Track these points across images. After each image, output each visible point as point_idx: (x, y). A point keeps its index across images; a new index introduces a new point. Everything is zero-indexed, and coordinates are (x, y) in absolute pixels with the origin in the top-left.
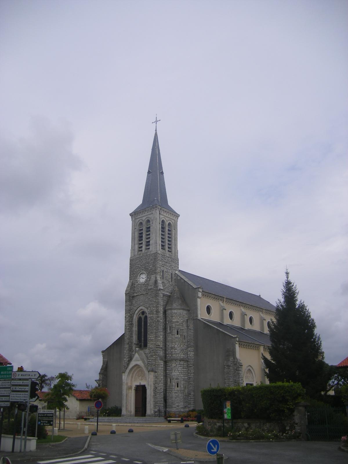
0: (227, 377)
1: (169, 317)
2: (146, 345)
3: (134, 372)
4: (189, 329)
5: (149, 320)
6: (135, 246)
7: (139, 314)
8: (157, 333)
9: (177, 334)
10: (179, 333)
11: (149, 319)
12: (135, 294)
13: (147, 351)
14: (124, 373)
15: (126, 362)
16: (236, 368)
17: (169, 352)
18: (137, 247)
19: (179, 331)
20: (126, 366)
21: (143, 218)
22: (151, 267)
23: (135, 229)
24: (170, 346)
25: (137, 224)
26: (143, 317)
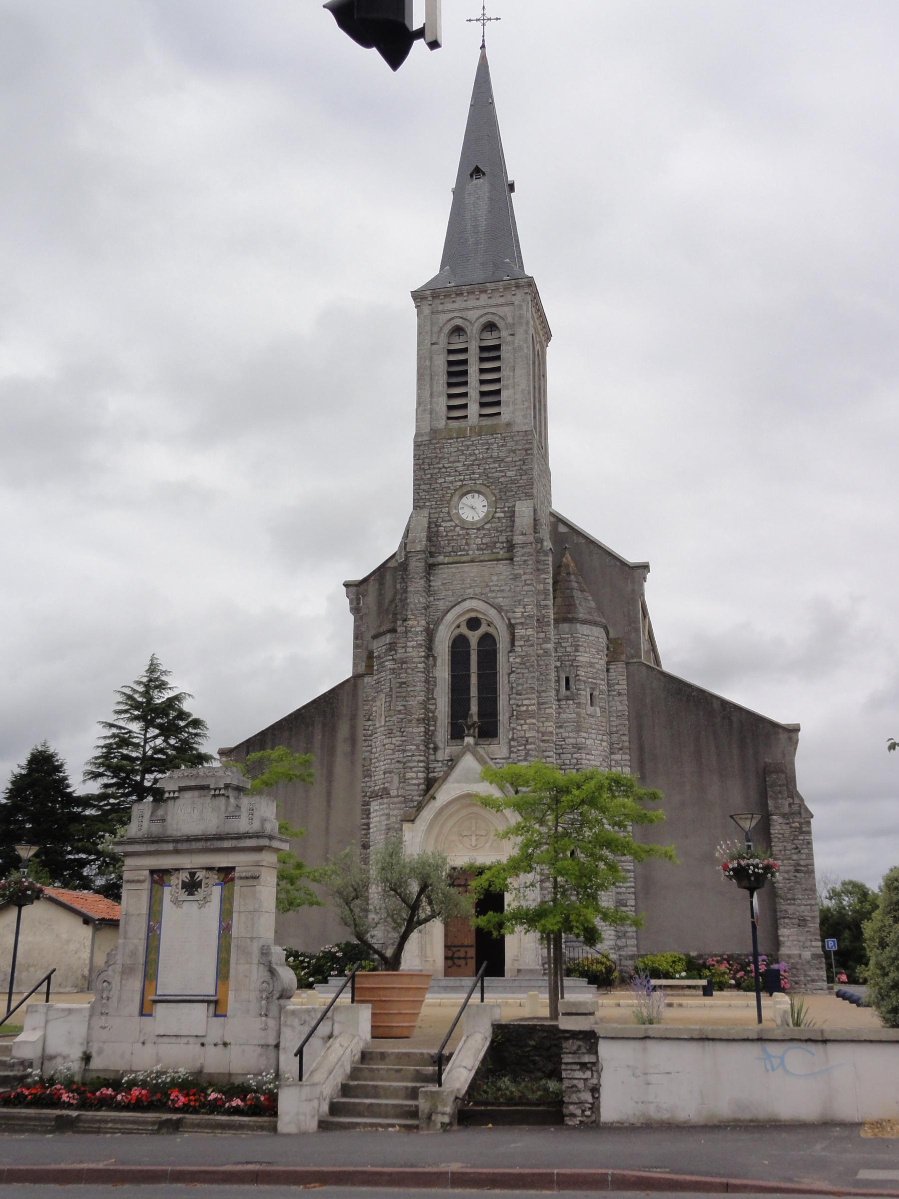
0: (780, 851)
1: (563, 645)
2: (488, 730)
3: (451, 816)
4: (614, 693)
5: (520, 646)
6: (435, 400)
7: (458, 626)
8: (544, 691)
9: (592, 705)
10: (596, 701)
11: (522, 643)
12: (441, 559)
13: (499, 749)
14: (413, 821)
15: (415, 785)
16: (797, 825)
17: (567, 762)
18: (442, 403)
19: (596, 693)
20: (417, 798)
21: (474, 311)
22: (509, 474)
23: (432, 344)
24: (569, 741)
25: (441, 329)
26: (474, 637)
